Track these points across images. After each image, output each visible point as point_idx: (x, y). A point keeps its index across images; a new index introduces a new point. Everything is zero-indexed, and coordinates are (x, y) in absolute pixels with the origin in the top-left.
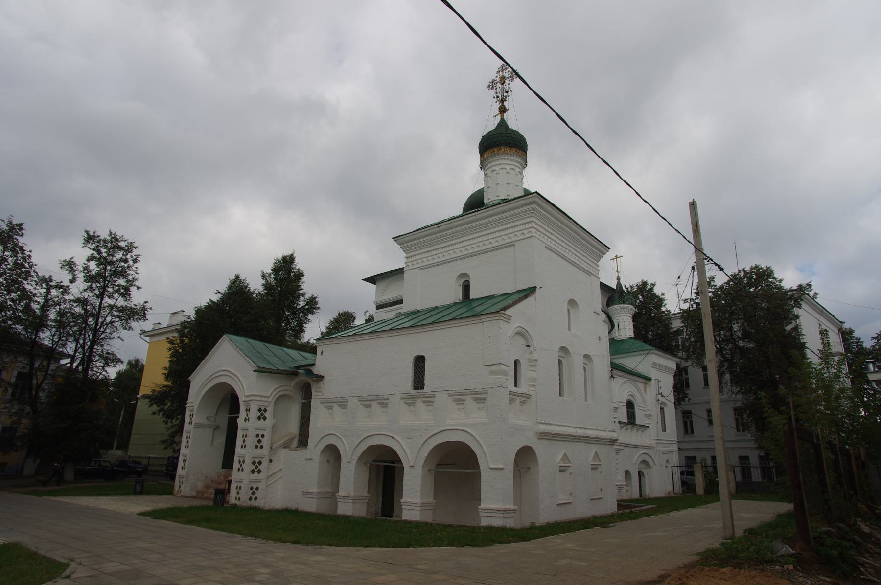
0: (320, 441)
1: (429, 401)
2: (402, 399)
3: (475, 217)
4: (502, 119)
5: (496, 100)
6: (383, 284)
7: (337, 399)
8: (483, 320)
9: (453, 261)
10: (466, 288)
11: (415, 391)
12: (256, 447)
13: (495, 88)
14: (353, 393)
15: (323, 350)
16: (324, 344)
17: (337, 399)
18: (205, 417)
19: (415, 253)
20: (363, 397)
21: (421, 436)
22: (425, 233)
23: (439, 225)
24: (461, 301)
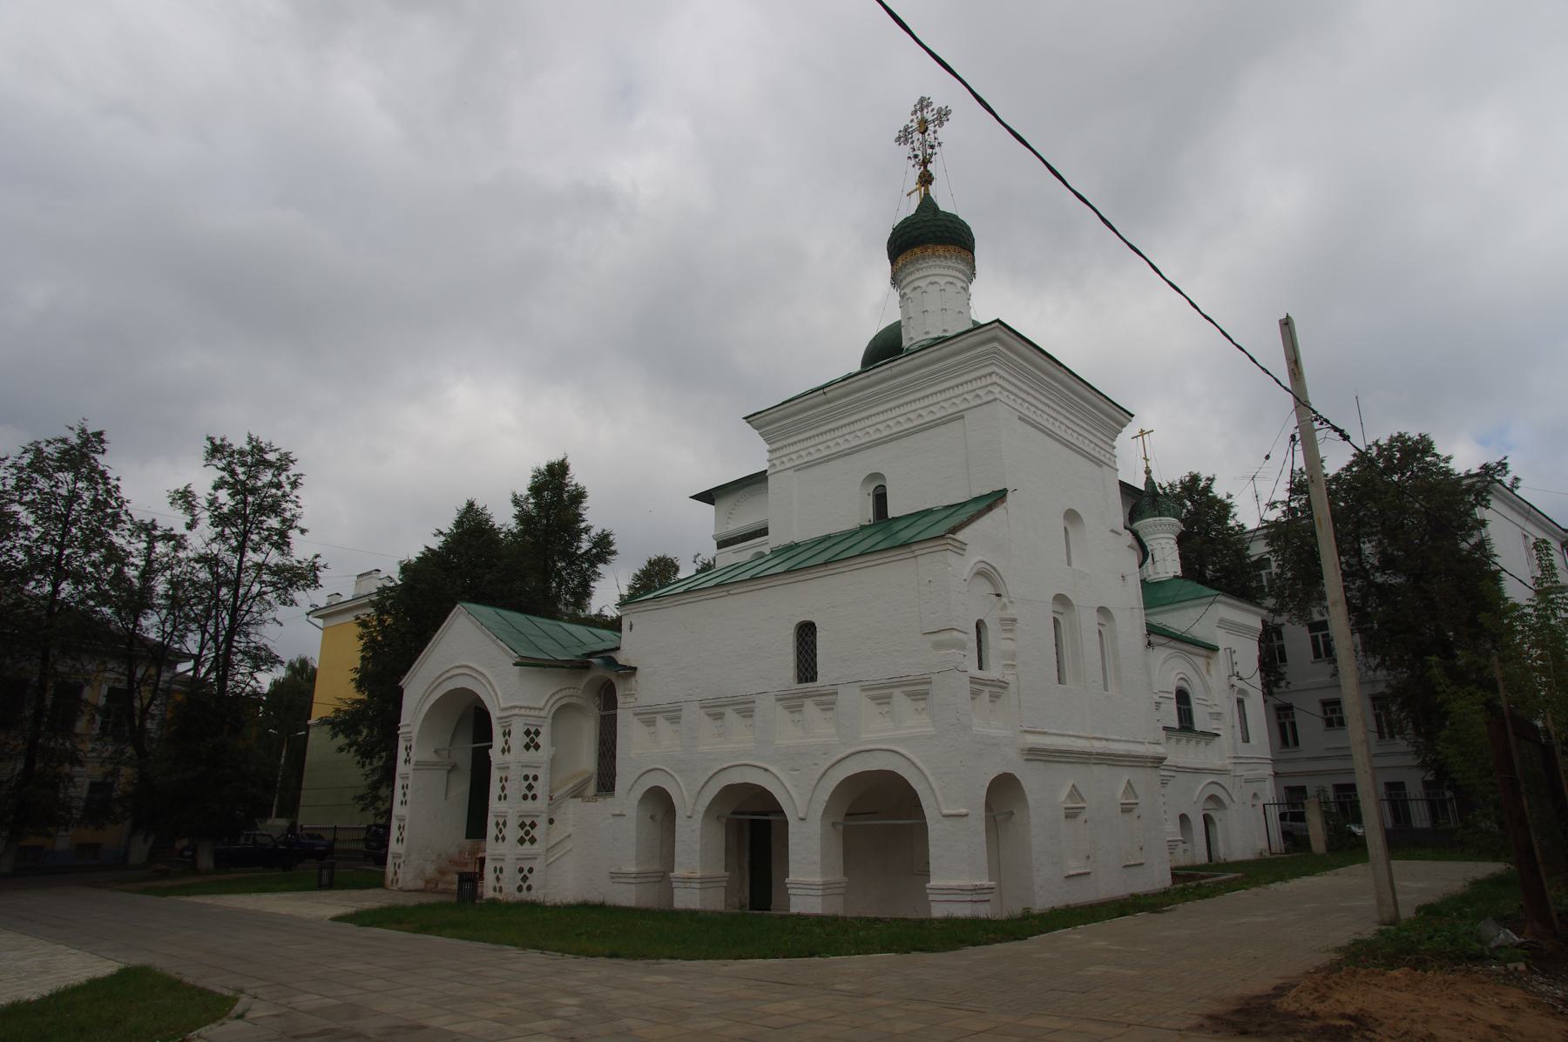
0: (636, 781)
1: (827, 702)
2: (778, 700)
5: (913, 162)
6: (727, 503)
8: (917, 553)
10: (880, 499)
12: (525, 797)
13: (910, 140)
15: (633, 622)
17: (663, 706)
18: (433, 750)
19: (785, 443)
20: (708, 701)
21: (816, 764)
22: (799, 406)
24: (872, 522)
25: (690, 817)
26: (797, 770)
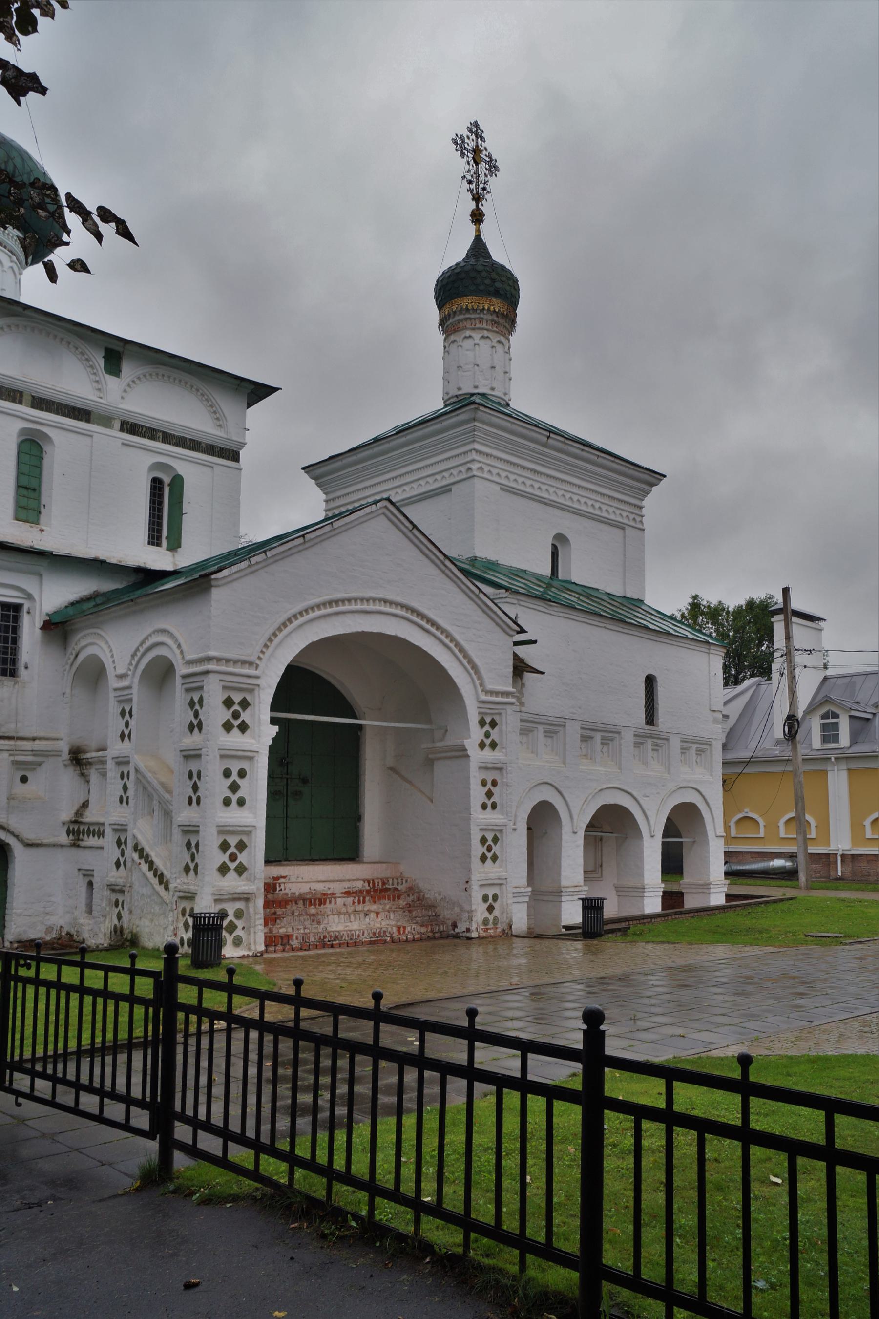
1: (660, 742)
3: (596, 458)
4: (478, 239)
8: (711, 651)
14: (574, 714)
16: (522, 603)
20: (588, 724)
21: (658, 793)
23: (552, 435)
26: (648, 796)
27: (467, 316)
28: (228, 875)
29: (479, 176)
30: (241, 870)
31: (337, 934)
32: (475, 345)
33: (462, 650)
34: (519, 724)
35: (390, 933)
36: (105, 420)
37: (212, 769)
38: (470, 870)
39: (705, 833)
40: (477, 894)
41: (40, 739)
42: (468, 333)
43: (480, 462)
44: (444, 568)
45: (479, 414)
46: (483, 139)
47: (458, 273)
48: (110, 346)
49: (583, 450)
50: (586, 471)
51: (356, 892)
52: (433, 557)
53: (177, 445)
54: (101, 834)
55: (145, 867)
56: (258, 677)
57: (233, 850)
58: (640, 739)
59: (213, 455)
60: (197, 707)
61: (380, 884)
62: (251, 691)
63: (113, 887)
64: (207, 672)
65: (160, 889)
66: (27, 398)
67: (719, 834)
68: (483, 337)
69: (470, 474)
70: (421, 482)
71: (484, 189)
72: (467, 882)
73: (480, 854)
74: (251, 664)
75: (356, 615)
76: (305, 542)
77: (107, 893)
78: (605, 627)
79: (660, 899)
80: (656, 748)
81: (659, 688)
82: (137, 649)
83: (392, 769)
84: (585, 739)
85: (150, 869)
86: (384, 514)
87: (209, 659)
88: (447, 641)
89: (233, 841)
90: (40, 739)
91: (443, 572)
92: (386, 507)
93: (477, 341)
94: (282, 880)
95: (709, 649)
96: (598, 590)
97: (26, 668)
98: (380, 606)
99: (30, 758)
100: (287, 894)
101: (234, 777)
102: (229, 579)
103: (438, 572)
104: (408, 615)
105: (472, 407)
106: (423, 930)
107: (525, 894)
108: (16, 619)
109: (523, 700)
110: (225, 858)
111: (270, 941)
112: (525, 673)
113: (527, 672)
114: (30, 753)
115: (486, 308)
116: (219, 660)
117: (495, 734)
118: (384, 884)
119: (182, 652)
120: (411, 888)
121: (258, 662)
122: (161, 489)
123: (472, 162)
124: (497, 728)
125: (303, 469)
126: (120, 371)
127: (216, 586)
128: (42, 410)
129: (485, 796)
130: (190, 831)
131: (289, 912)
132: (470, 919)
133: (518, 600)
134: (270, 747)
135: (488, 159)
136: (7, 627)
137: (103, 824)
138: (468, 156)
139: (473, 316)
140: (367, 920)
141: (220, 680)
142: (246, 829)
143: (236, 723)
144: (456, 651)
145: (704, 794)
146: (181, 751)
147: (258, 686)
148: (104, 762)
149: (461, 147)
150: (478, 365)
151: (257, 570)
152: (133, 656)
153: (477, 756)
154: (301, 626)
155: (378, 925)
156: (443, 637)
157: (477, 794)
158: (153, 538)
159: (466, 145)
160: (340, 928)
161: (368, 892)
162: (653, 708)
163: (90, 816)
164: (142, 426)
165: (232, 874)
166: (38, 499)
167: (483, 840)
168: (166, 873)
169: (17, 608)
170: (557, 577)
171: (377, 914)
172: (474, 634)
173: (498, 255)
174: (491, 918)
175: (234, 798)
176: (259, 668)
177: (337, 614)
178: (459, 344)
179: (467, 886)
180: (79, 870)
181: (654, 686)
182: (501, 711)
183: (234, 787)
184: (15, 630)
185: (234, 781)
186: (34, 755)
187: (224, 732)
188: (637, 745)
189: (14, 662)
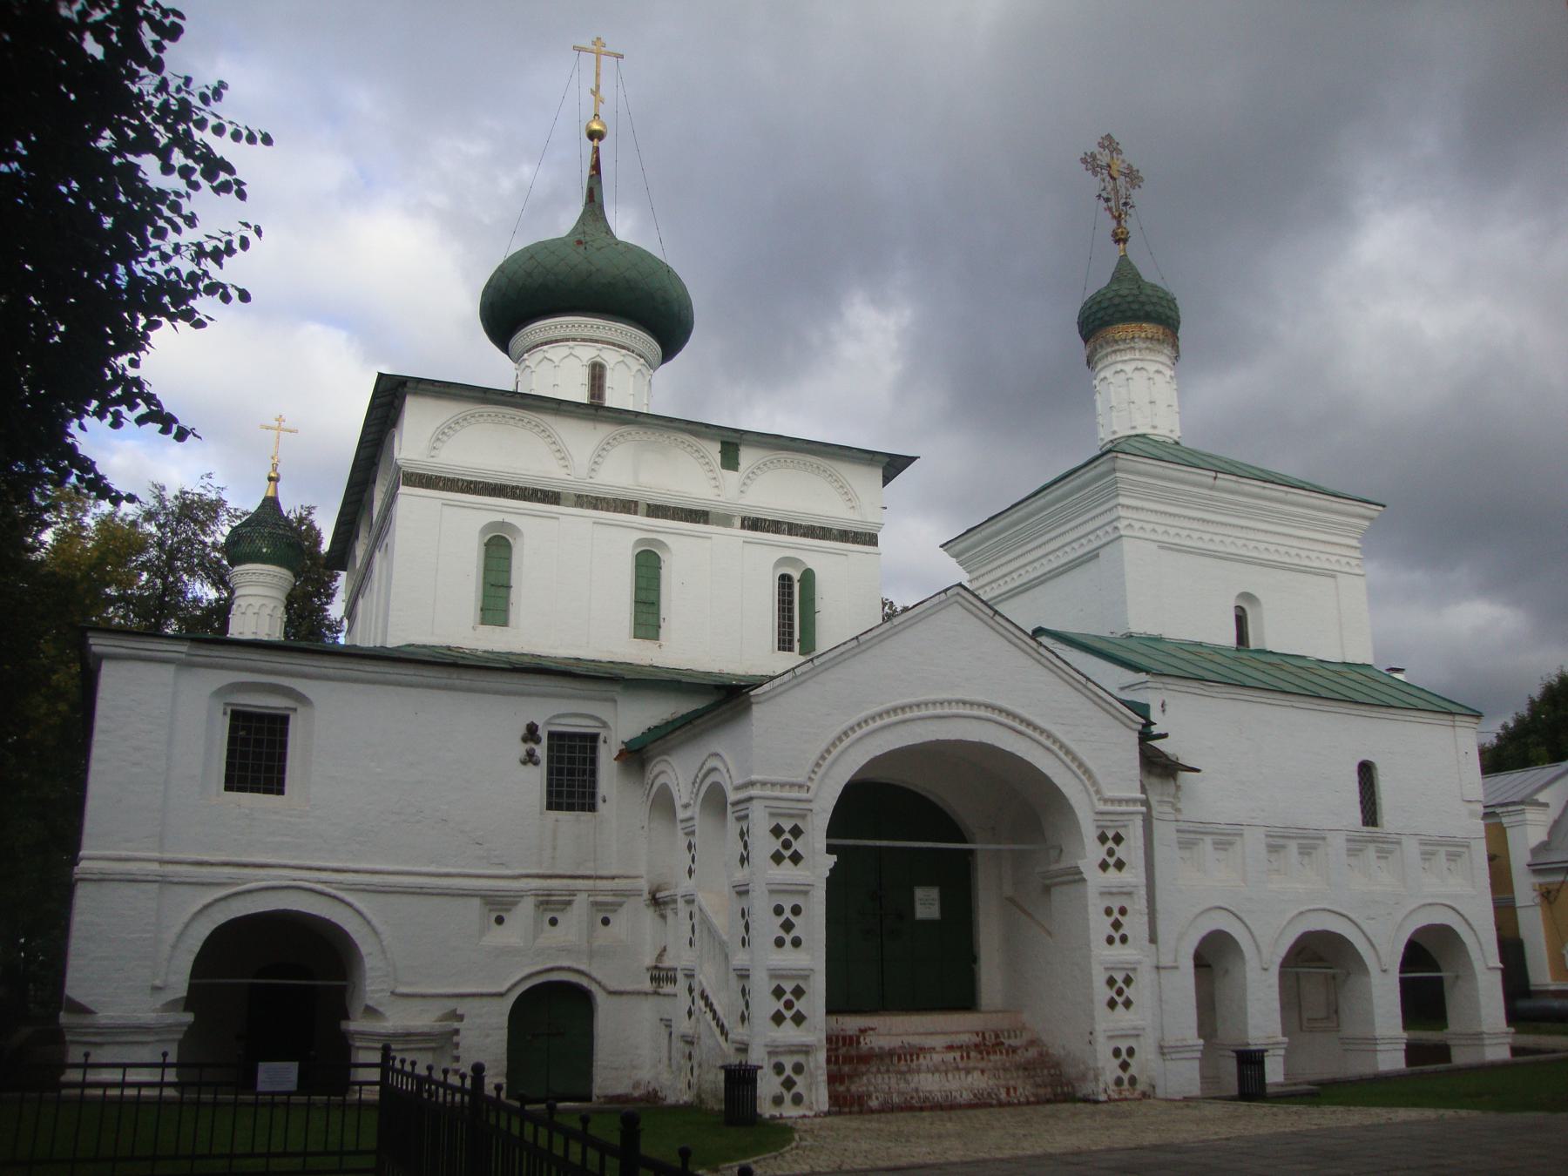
1: (1388, 847)
7: (1220, 826)
8: (1457, 723)
9: (1231, 560)
11: (1366, 829)
14: (1253, 818)
15: (1167, 702)
16: (1170, 687)
17: (1220, 826)
20: (1276, 829)
23: (1219, 475)
25: (1266, 970)
26: (1374, 919)
27: (1116, 347)
28: (784, 1024)
29: (1118, 192)
30: (799, 1019)
31: (928, 1095)
32: (1128, 379)
33: (1068, 752)
34: (1175, 836)
35: (996, 1095)
36: (725, 520)
37: (761, 906)
38: (1093, 1018)
39: (1469, 964)
40: (1104, 1050)
41: (619, 877)
42: (1119, 367)
43: (1128, 518)
44: (1038, 657)
45: (1119, 464)
46: (1120, 152)
47: (1100, 302)
48: (726, 439)
49: (1264, 488)
50: (1271, 511)
51: (962, 1046)
52: (1023, 646)
53: (805, 535)
54: (674, 980)
55: (709, 1016)
56: (810, 801)
57: (788, 996)
58: (1355, 847)
59: (847, 541)
60: (746, 838)
61: (993, 1037)
62: (803, 817)
63: (686, 1039)
64: (750, 799)
65: (721, 1040)
66: (642, 508)
67: (1491, 965)
68: (1136, 369)
69: (1116, 535)
70: (1067, 549)
71: (1125, 204)
72: (1091, 1033)
73: (1107, 998)
74: (801, 786)
75: (928, 722)
76: (859, 645)
77: (681, 1045)
78: (1293, 707)
79: (1403, 1054)
80: (1383, 855)
81: (1380, 777)
82: (697, 776)
83: (1011, 900)
84: (1274, 849)
85: (714, 1018)
86: (957, 602)
87: (752, 784)
88: (1048, 743)
89: (788, 986)
90: (619, 877)
91: (1039, 662)
92: (958, 594)
93: (1130, 375)
94: (871, 1032)
95: (1454, 721)
96: (1303, 657)
97: (604, 801)
98: (958, 709)
99: (610, 899)
100: (872, 1048)
101: (787, 914)
102: (771, 694)
103: (1030, 662)
104: (996, 716)
105: (1110, 455)
106: (1041, 1091)
107: (1195, 1048)
108: (594, 749)
109: (1179, 805)
110: (780, 1005)
111: (834, 1099)
112: (1180, 772)
113: (1182, 770)
114: (611, 893)
115: (1136, 335)
116: (764, 784)
117: (1121, 851)
118: (997, 1036)
119: (730, 777)
120: (1032, 1043)
121: (809, 784)
122: (791, 587)
123: (1108, 178)
124: (1123, 845)
125: (942, 546)
126: (738, 464)
127: (757, 703)
128: (657, 517)
129: (1111, 929)
130: (744, 975)
131: (874, 1069)
132: (1096, 1079)
133: (1163, 683)
134: (828, 880)
135: (1127, 172)
136: (585, 759)
137: (676, 969)
138: (1102, 174)
139: (1122, 347)
140: (970, 1079)
141: (766, 807)
142: (802, 972)
143: (787, 853)
144: (1062, 754)
145: (1462, 912)
146: (734, 887)
147: (811, 810)
148: (675, 901)
149: (1093, 165)
150: (1133, 403)
151: (803, 682)
152: (694, 784)
153: (1096, 879)
154: (860, 739)
155: (984, 1085)
156: (1042, 739)
157: (1100, 926)
158: (784, 641)
159: (1098, 162)
160: (935, 1087)
161: (976, 1046)
162: (1374, 804)
163: (667, 963)
164: (765, 520)
165: (788, 1024)
166: (657, 613)
167: (1111, 982)
168: (726, 1024)
169: (594, 738)
170: (1248, 647)
171: (983, 1072)
172: (1085, 733)
173: (1149, 275)
174: (1126, 1077)
175: (788, 938)
176: (810, 791)
177: (904, 722)
178: (1109, 381)
179: (1091, 1037)
180: (661, 1020)
181: (1374, 775)
182: (1126, 823)
183: (787, 926)
184: (593, 761)
185: (787, 918)
186: (614, 895)
187: (773, 864)
188: (1352, 853)
189: (593, 795)
